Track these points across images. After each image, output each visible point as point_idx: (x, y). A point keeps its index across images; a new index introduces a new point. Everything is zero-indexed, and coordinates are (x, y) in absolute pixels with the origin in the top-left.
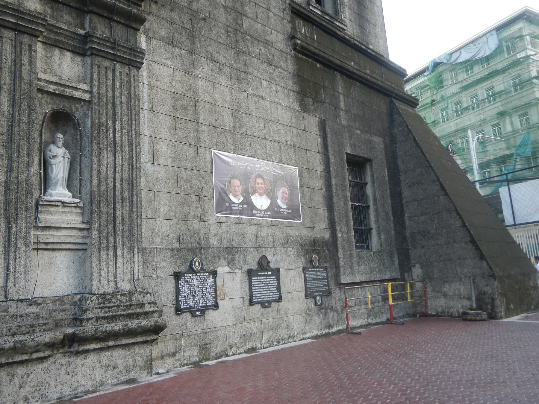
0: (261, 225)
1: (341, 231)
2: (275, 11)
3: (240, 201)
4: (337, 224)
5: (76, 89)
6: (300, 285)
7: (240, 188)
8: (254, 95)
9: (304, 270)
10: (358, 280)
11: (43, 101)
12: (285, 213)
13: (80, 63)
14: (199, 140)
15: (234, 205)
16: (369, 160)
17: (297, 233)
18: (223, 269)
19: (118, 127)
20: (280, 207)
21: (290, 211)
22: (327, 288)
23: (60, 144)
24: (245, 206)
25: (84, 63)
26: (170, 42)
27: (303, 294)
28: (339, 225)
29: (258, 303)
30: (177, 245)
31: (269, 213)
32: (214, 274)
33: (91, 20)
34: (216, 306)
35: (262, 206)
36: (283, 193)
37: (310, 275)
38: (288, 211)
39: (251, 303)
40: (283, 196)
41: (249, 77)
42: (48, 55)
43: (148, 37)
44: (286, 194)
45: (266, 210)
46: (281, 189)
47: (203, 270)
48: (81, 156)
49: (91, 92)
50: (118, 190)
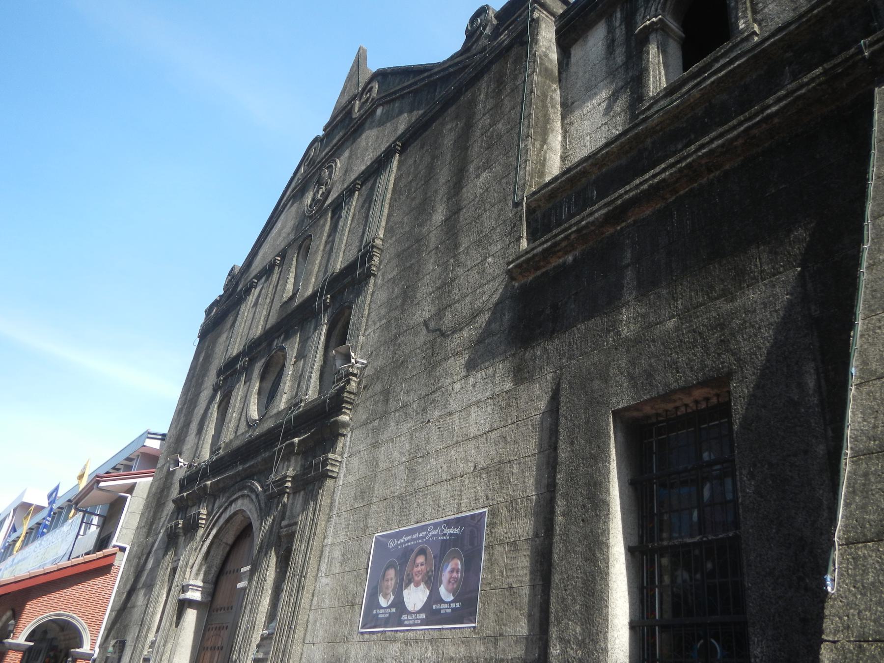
0: (407, 643)
1: (561, 640)
3: (390, 602)
4: (552, 618)
7: (393, 582)
12: (448, 611)
15: (381, 611)
17: (463, 651)
19: (303, 548)
20: (442, 601)
21: (458, 605)
24: (393, 610)
28: (559, 623)
31: (423, 616)
35: (415, 604)
36: (452, 571)
38: (453, 605)
40: (451, 578)
43: (352, 432)
44: (457, 572)
45: (420, 612)
46: (450, 564)
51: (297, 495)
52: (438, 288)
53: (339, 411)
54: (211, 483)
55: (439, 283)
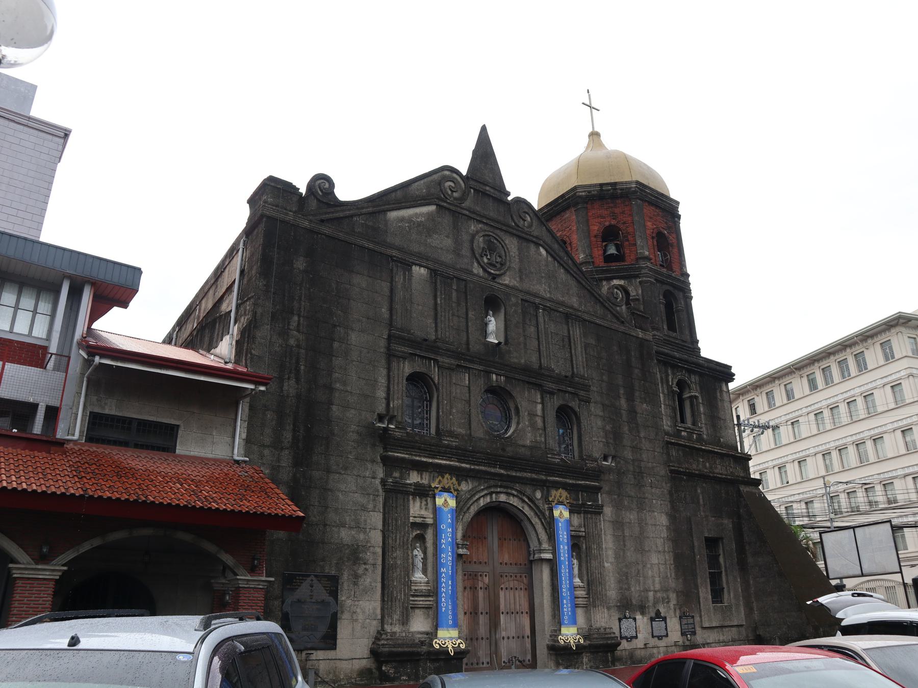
2: (658, 450)
5: (580, 531)
6: (678, 627)
8: (649, 511)
9: (680, 618)
10: (714, 625)
14: (625, 546)
16: (722, 539)
18: (639, 617)
22: (693, 630)
26: (609, 493)
27: (680, 633)
29: (656, 636)
30: (619, 604)
32: (635, 619)
33: (582, 495)
34: (636, 637)
37: (684, 621)
39: (653, 637)
41: (647, 500)
43: (601, 495)
47: (630, 618)
49: (585, 532)
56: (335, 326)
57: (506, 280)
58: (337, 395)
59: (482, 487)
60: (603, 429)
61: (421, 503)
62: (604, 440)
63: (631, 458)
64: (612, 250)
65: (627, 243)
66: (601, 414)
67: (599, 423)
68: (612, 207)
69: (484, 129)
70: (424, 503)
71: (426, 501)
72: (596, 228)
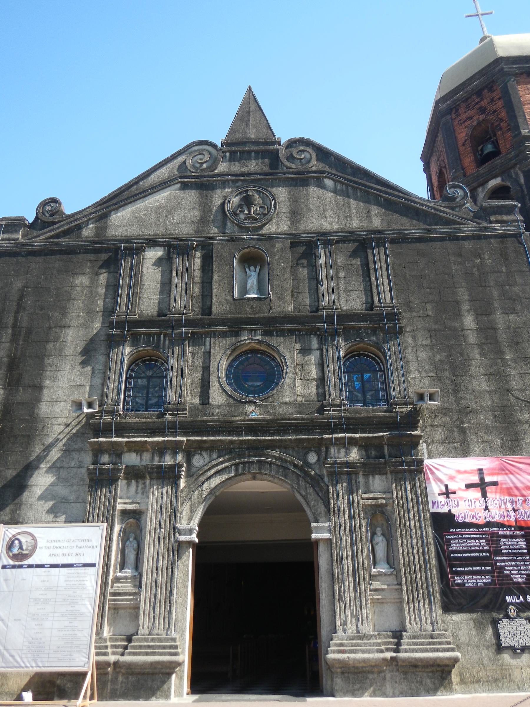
11: (367, 510)
13: (385, 480)
19: (412, 517)
23: (379, 534)
25: (387, 478)
42: (366, 481)
43: (428, 445)
48: (392, 540)
50: (417, 560)
51: (371, 478)
52: (492, 374)
53: (415, 428)
54: (187, 440)
55: (491, 370)
56: (50, 328)
57: (270, 228)
58: (46, 391)
59: (221, 459)
60: (431, 361)
61: (137, 487)
62: (432, 374)
63: (487, 388)
64: (489, 148)
65: (499, 133)
66: (428, 342)
67: (423, 355)
68: (477, 103)
69: (250, 88)
70: (141, 486)
71: (144, 484)
72: (464, 134)
